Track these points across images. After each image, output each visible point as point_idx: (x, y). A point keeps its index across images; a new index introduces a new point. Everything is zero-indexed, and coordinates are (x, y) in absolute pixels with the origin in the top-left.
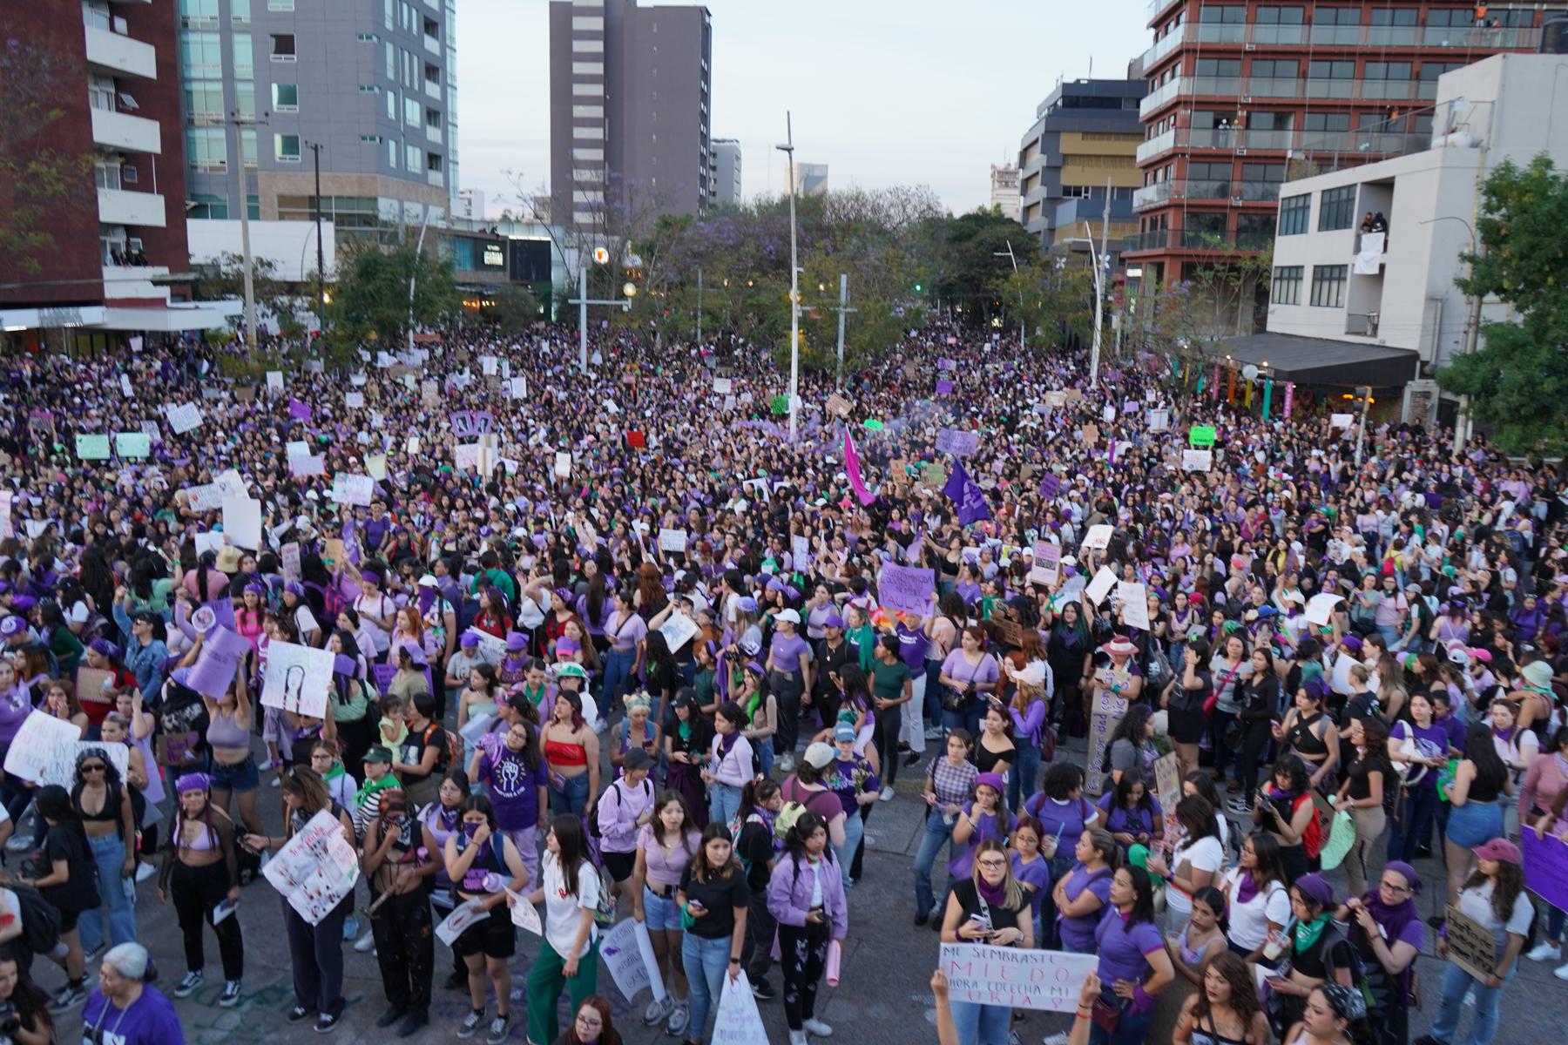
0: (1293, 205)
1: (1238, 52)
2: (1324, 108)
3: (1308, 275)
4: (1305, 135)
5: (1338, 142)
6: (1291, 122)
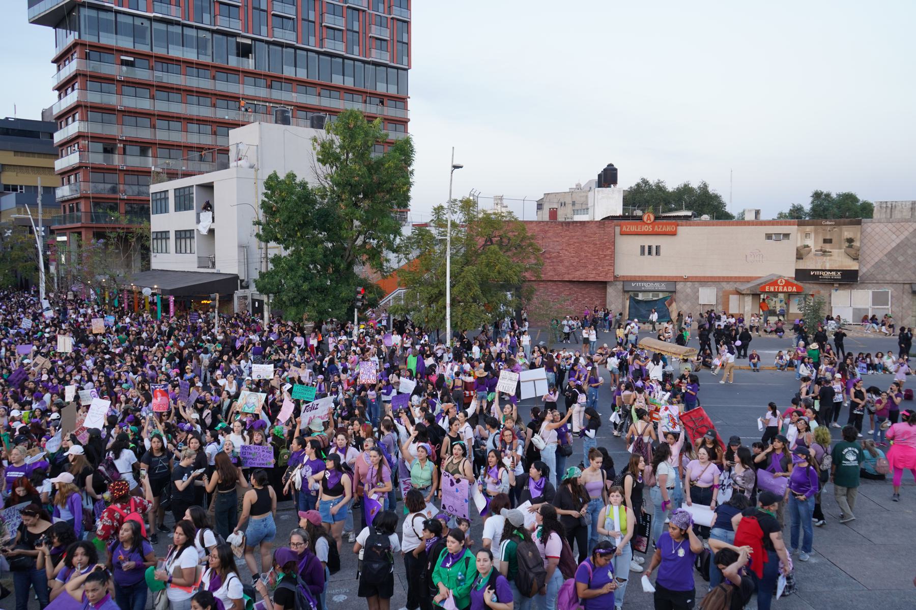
0: (158, 197)
1: (114, 110)
2: (169, 146)
3: (172, 236)
4: (160, 161)
6: (150, 153)
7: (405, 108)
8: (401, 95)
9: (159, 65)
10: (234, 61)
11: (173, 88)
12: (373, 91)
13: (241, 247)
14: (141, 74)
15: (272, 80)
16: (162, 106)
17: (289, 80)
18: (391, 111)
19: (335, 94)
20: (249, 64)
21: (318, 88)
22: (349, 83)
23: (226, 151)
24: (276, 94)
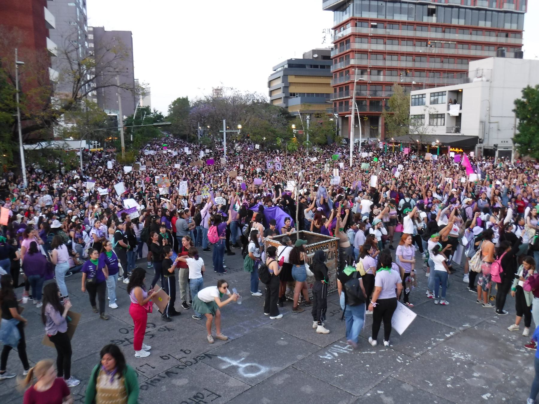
0: (417, 97)
2: (391, 69)
4: (387, 77)
5: (436, 81)
6: (382, 73)
7: (521, 38)
8: (519, 30)
9: (388, 26)
10: (426, 19)
11: (396, 38)
12: (502, 29)
13: (481, 122)
14: (380, 31)
15: (446, 27)
16: (389, 48)
17: (455, 27)
18: (511, 40)
19: (480, 32)
20: (433, 20)
21: (470, 30)
22: (488, 25)
23: (466, 72)
24: (448, 36)
